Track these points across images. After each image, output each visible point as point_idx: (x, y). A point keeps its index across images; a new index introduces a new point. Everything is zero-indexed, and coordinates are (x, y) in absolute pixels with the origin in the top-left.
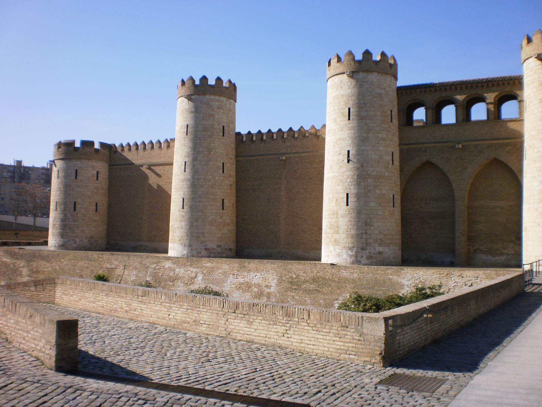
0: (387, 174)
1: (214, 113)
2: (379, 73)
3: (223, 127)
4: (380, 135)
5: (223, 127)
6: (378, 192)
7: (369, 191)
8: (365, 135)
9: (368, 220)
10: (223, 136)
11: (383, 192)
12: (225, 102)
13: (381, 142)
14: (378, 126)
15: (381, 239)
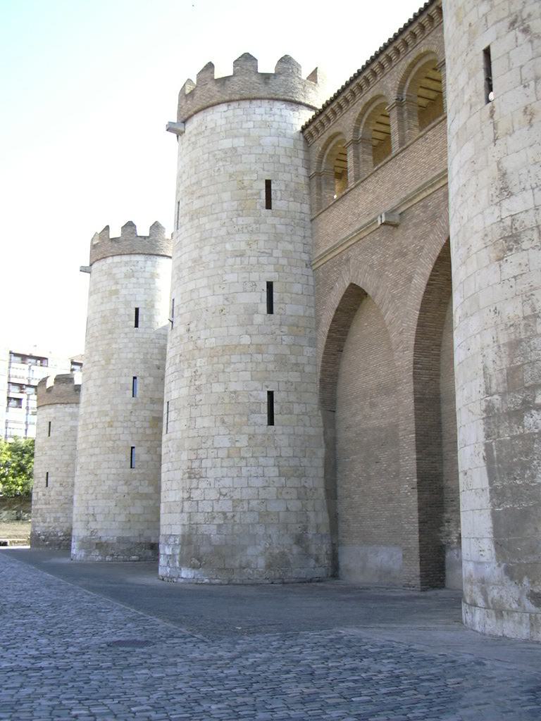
0: (246, 340)
1: (119, 287)
2: (229, 102)
3: (137, 310)
4: (228, 247)
5: (137, 310)
6: (218, 388)
7: (198, 388)
8: (195, 254)
9: (196, 464)
10: (136, 326)
11: (232, 387)
12: (141, 264)
13: (231, 261)
14: (223, 225)
15: (224, 513)
